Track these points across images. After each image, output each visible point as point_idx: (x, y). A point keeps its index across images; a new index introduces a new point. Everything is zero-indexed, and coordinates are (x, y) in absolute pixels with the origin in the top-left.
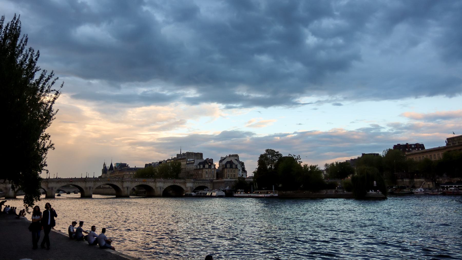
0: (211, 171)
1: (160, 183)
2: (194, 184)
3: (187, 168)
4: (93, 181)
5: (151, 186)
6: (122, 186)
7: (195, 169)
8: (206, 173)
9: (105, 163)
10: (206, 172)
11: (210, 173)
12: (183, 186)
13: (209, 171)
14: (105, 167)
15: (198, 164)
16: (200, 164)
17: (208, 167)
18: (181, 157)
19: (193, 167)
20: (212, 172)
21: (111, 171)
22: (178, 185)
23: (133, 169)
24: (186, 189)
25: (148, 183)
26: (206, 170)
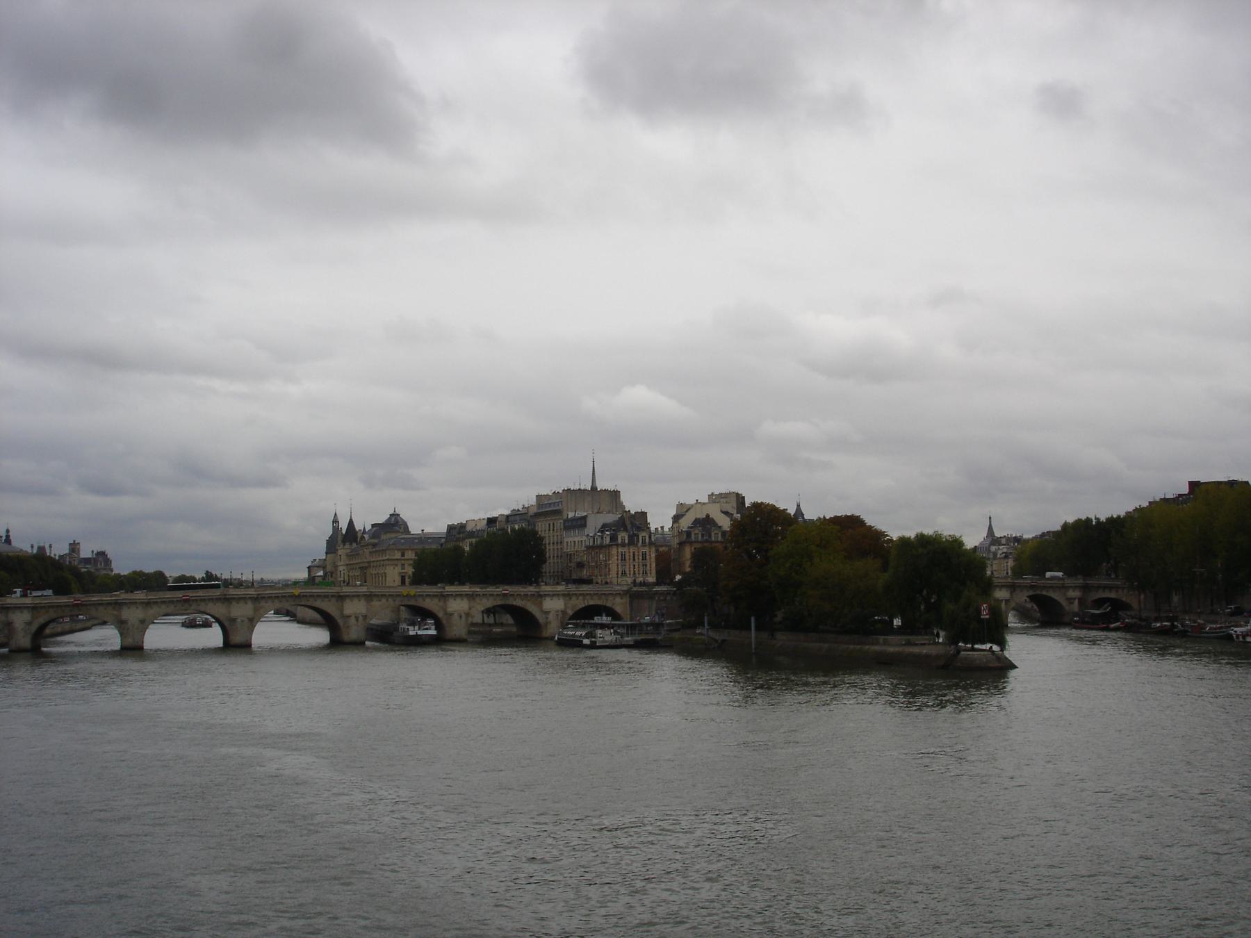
0: (636, 554)
1: (458, 600)
2: (567, 598)
3: (566, 540)
4: (250, 598)
5: (430, 609)
6: (342, 610)
7: (588, 548)
8: (622, 560)
9: (336, 514)
10: (620, 558)
11: (634, 560)
12: (532, 608)
13: (631, 550)
14: (336, 529)
15: (597, 530)
16: (605, 527)
17: (627, 541)
18: (549, 508)
19: (584, 538)
20: (641, 558)
21: (351, 544)
22: (518, 603)
23: (415, 538)
24: (544, 616)
25: (420, 600)
26: (620, 550)
